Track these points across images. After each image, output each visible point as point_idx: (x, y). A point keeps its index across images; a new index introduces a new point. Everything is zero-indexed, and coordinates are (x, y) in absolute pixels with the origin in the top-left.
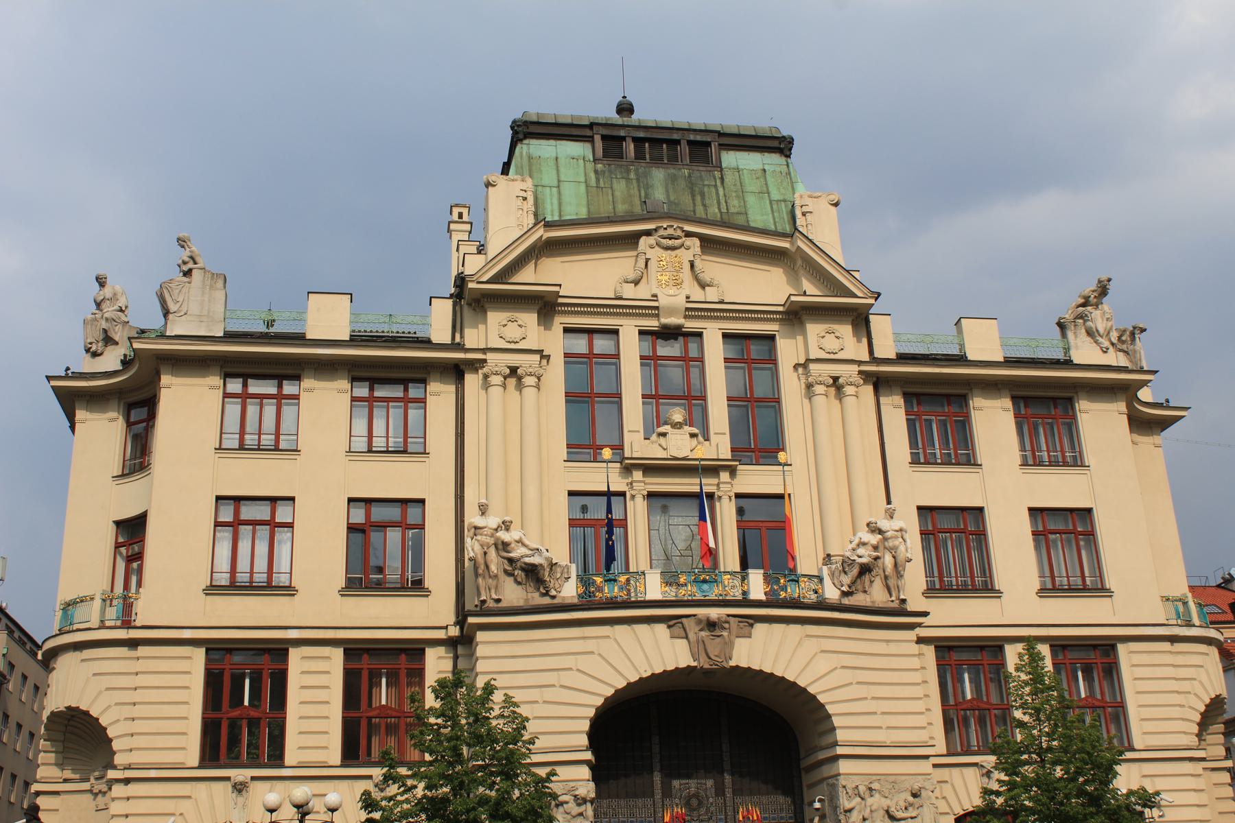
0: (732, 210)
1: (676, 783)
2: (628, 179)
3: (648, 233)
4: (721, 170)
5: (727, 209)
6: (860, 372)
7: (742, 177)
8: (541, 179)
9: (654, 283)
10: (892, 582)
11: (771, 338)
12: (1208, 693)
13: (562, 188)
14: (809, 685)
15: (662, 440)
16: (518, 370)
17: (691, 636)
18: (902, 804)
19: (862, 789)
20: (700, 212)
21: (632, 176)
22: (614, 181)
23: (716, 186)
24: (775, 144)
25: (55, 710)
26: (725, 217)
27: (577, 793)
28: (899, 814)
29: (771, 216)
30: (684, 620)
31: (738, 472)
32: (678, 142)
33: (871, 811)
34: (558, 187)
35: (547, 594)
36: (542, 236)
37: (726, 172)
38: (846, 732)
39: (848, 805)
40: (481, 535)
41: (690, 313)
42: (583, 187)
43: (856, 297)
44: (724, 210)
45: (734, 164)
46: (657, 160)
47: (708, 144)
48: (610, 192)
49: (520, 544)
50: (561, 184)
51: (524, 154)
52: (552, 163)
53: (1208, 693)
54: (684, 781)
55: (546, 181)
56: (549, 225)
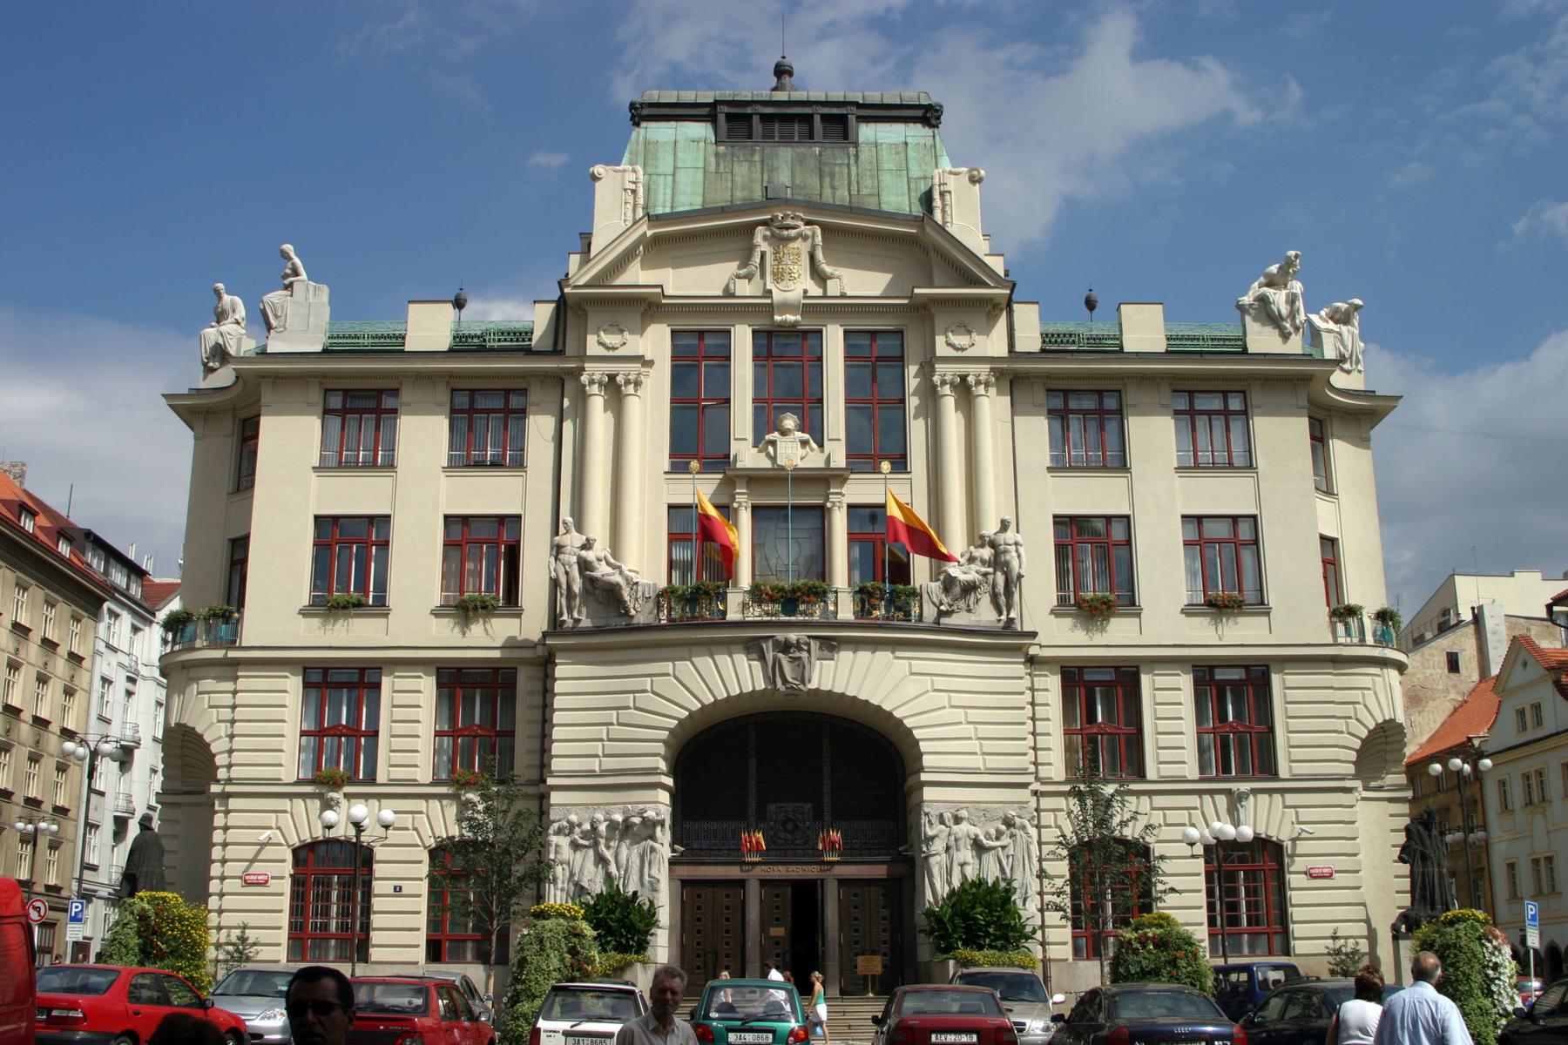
0: (864, 192)
1: (772, 807)
2: (751, 162)
3: (764, 223)
4: (856, 144)
5: (858, 191)
6: (991, 369)
7: (880, 153)
8: (656, 167)
9: (769, 277)
10: (1002, 600)
11: (900, 333)
12: (1383, 714)
13: (677, 175)
14: (895, 708)
15: (771, 449)
16: (618, 378)
17: (770, 657)
18: (993, 832)
19: (947, 816)
21: (757, 157)
22: (736, 164)
23: (848, 164)
24: (919, 113)
26: (855, 200)
27: (645, 815)
28: (986, 842)
29: (907, 196)
31: (849, 482)
32: (808, 119)
33: (956, 840)
34: (674, 175)
36: (645, 233)
37: (862, 148)
38: (935, 758)
39: (930, 833)
41: (808, 309)
42: (700, 175)
43: (987, 286)
44: (854, 192)
45: (872, 139)
46: (787, 140)
47: (843, 119)
48: (729, 177)
49: (604, 562)
50: (677, 171)
51: (641, 138)
52: (670, 149)
53: (1383, 714)
54: (779, 805)
55: (661, 170)
56: (654, 219)
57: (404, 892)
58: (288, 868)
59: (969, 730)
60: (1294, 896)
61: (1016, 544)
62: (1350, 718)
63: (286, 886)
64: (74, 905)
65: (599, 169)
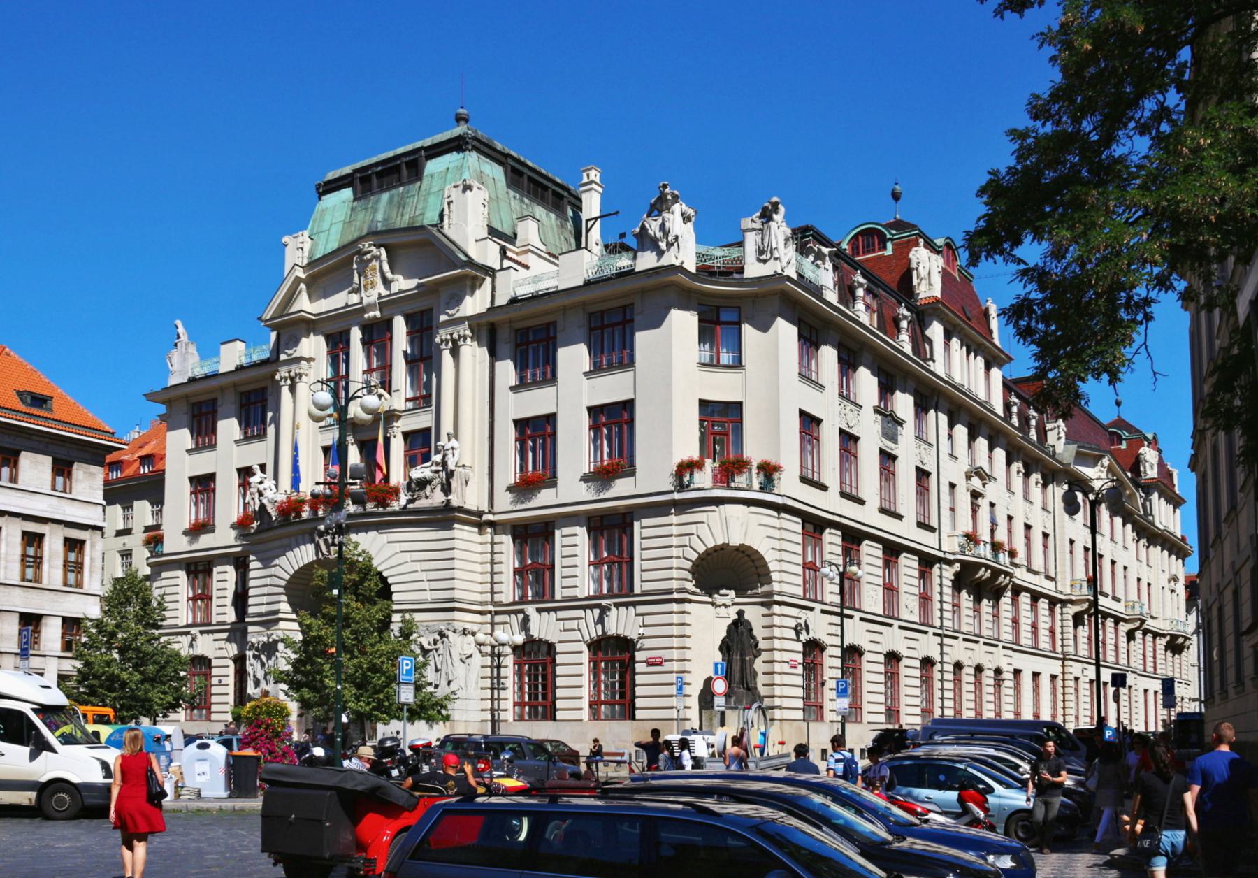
2: (366, 209)
20: (397, 226)
59: (424, 576)
60: (639, 679)
61: (453, 449)
62: (685, 546)
65: (286, 239)
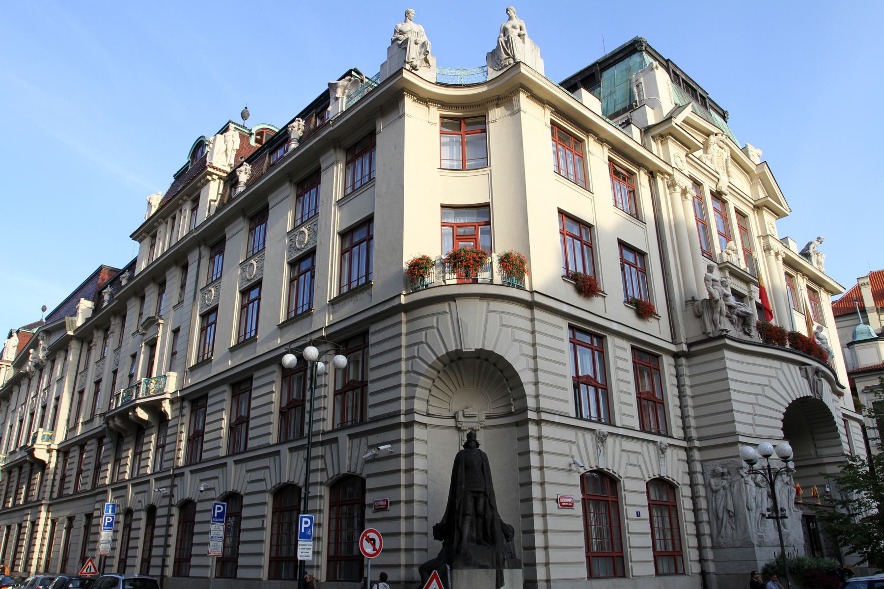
25: (464, 350)
30: (808, 367)
35: (749, 335)
40: (718, 286)
57: (642, 516)
58: (577, 494)
63: (578, 509)
64: (304, 520)
